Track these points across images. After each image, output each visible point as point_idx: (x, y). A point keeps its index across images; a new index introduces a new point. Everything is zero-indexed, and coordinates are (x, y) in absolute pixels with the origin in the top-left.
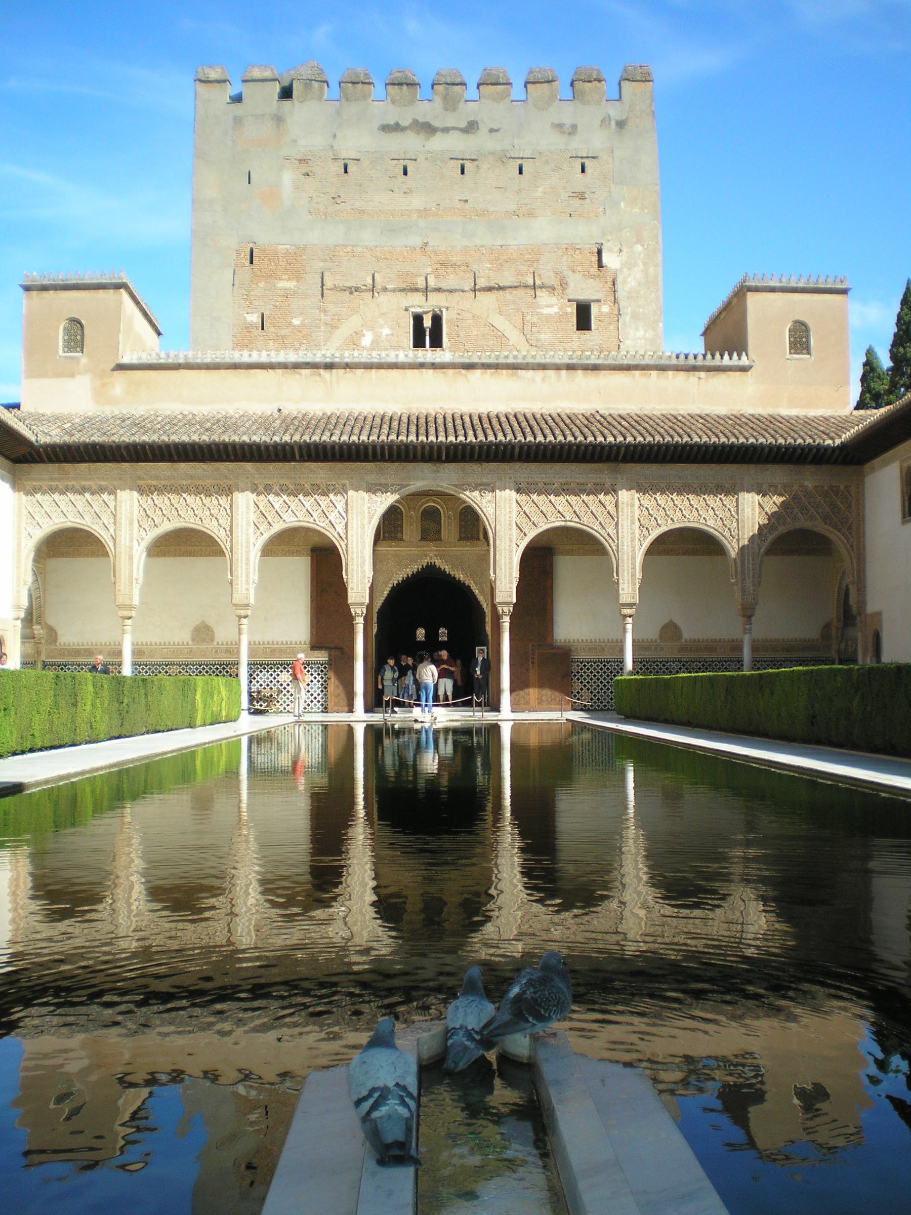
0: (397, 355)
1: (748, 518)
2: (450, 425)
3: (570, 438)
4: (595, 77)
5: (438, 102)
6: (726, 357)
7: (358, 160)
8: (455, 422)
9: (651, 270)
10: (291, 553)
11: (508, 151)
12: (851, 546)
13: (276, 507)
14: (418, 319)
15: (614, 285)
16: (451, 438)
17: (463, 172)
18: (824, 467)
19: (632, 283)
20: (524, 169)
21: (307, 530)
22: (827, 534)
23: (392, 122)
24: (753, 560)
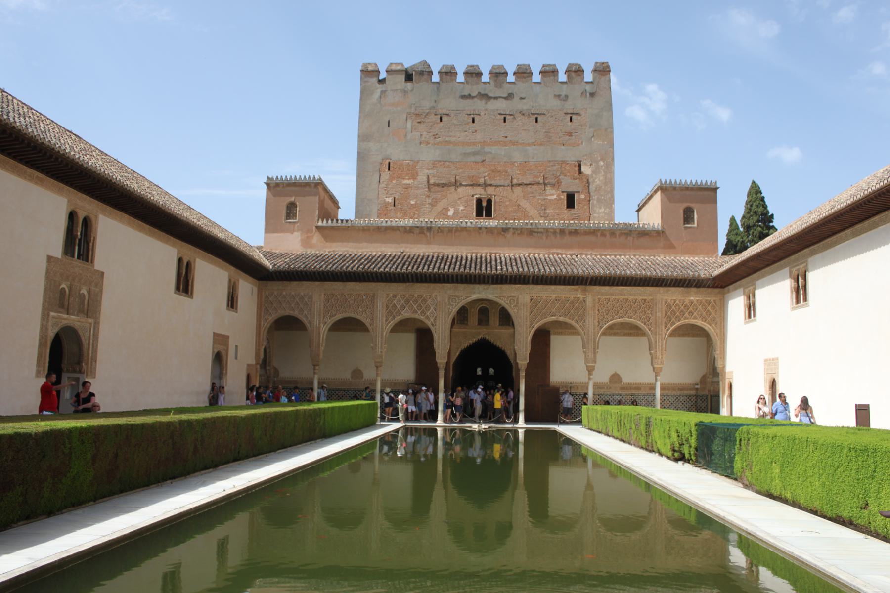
2: (494, 263)
5: (492, 83)
7: (447, 115)
10: (407, 331)
11: (530, 110)
13: (398, 307)
14: (479, 201)
15: (588, 182)
16: (494, 272)
17: (505, 121)
18: (701, 289)
19: (597, 182)
20: (538, 120)
21: (415, 319)
22: (704, 327)
23: (466, 93)
24: (661, 340)
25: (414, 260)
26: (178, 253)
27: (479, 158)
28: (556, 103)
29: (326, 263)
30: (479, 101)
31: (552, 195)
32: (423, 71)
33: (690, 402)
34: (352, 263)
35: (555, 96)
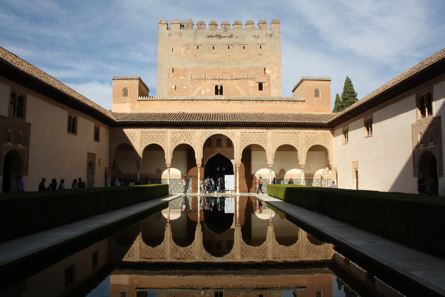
0: (210, 97)
1: (303, 142)
2: (223, 117)
3: (255, 121)
4: (264, 23)
6: (298, 99)
7: (202, 45)
8: (225, 115)
9: (279, 74)
12: (330, 150)
14: (216, 87)
16: (224, 121)
17: (229, 48)
19: (273, 78)
23: (210, 35)
24: (304, 153)
25: (185, 116)
26: (69, 113)
27: (216, 66)
28: (254, 40)
29: (143, 117)
30: (216, 38)
31: (252, 84)
32: (189, 24)
33: (318, 182)
34: (155, 118)
35: (253, 36)
